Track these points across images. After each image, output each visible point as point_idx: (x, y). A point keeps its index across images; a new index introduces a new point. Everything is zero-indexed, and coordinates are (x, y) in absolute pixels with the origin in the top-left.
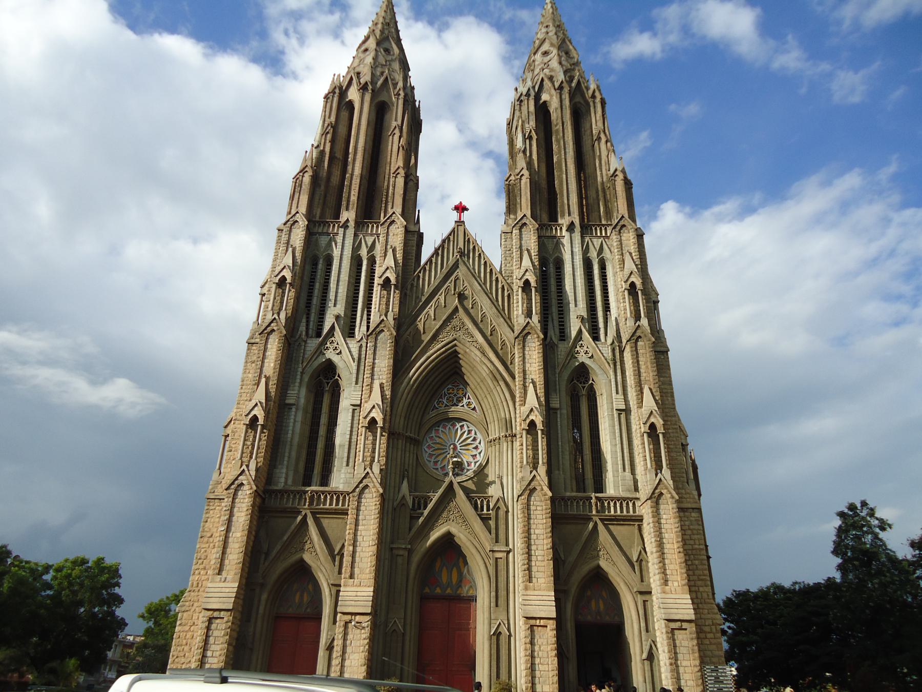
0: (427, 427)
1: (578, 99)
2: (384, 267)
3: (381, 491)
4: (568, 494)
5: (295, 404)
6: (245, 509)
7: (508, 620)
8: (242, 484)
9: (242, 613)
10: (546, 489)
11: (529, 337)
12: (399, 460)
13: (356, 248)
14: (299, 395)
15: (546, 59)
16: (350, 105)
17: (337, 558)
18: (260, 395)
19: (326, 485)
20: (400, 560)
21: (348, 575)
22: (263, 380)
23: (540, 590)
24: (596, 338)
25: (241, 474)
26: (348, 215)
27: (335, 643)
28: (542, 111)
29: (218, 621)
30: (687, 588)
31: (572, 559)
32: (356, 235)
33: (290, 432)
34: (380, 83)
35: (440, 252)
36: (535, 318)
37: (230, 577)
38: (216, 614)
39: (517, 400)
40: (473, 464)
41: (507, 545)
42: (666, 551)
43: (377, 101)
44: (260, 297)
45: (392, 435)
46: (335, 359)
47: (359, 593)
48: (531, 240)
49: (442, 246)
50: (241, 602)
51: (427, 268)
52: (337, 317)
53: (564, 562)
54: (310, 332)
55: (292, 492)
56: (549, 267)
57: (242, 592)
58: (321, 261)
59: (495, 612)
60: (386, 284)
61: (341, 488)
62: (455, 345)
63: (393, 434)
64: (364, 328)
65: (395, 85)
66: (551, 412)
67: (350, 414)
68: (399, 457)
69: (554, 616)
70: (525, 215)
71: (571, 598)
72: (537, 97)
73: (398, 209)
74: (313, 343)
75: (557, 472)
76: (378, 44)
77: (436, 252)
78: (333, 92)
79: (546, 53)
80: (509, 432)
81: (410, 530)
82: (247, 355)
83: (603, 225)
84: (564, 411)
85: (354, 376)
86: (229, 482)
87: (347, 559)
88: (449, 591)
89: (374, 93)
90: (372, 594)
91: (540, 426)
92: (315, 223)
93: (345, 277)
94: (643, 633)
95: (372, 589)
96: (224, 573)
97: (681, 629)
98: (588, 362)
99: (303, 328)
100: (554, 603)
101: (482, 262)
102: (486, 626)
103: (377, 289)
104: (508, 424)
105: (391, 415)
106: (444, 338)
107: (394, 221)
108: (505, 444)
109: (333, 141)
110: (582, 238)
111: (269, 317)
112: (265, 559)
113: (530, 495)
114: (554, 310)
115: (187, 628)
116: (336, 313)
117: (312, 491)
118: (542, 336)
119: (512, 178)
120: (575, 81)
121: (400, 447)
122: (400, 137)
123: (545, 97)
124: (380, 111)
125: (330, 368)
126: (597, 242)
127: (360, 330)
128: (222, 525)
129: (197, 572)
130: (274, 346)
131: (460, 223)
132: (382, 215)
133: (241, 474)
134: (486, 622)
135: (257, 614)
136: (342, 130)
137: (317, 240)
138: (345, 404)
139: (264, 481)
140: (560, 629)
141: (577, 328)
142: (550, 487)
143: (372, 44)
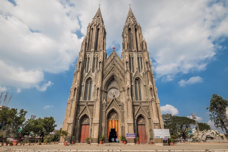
4: (135, 101)
5: (84, 85)
7: (124, 124)
8: (74, 100)
10: (131, 100)
13: (94, 56)
15: (130, 20)
18: (76, 84)
20: (104, 114)
22: (77, 81)
24: (140, 72)
26: (93, 50)
28: (130, 29)
41: (124, 110)
45: (102, 91)
46: (91, 77)
47: (96, 119)
48: (127, 54)
52: (91, 69)
58: (87, 59)
61: (93, 101)
64: (96, 71)
69: (133, 123)
72: (128, 27)
73: (102, 49)
78: (89, 26)
79: (130, 19)
81: (106, 107)
84: (134, 86)
89: (97, 27)
91: (130, 88)
93: (92, 61)
97: (156, 125)
101: (118, 58)
104: (124, 88)
106: (111, 73)
109: (89, 36)
110: (137, 53)
111: (78, 69)
114: (132, 67)
123: (130, 27)
125: (90, 78)
126: (140, 55)
127: (96, 71)
136: (91, 34)
138: (93, 85)
140: (134, 125)
143: (96, 17)
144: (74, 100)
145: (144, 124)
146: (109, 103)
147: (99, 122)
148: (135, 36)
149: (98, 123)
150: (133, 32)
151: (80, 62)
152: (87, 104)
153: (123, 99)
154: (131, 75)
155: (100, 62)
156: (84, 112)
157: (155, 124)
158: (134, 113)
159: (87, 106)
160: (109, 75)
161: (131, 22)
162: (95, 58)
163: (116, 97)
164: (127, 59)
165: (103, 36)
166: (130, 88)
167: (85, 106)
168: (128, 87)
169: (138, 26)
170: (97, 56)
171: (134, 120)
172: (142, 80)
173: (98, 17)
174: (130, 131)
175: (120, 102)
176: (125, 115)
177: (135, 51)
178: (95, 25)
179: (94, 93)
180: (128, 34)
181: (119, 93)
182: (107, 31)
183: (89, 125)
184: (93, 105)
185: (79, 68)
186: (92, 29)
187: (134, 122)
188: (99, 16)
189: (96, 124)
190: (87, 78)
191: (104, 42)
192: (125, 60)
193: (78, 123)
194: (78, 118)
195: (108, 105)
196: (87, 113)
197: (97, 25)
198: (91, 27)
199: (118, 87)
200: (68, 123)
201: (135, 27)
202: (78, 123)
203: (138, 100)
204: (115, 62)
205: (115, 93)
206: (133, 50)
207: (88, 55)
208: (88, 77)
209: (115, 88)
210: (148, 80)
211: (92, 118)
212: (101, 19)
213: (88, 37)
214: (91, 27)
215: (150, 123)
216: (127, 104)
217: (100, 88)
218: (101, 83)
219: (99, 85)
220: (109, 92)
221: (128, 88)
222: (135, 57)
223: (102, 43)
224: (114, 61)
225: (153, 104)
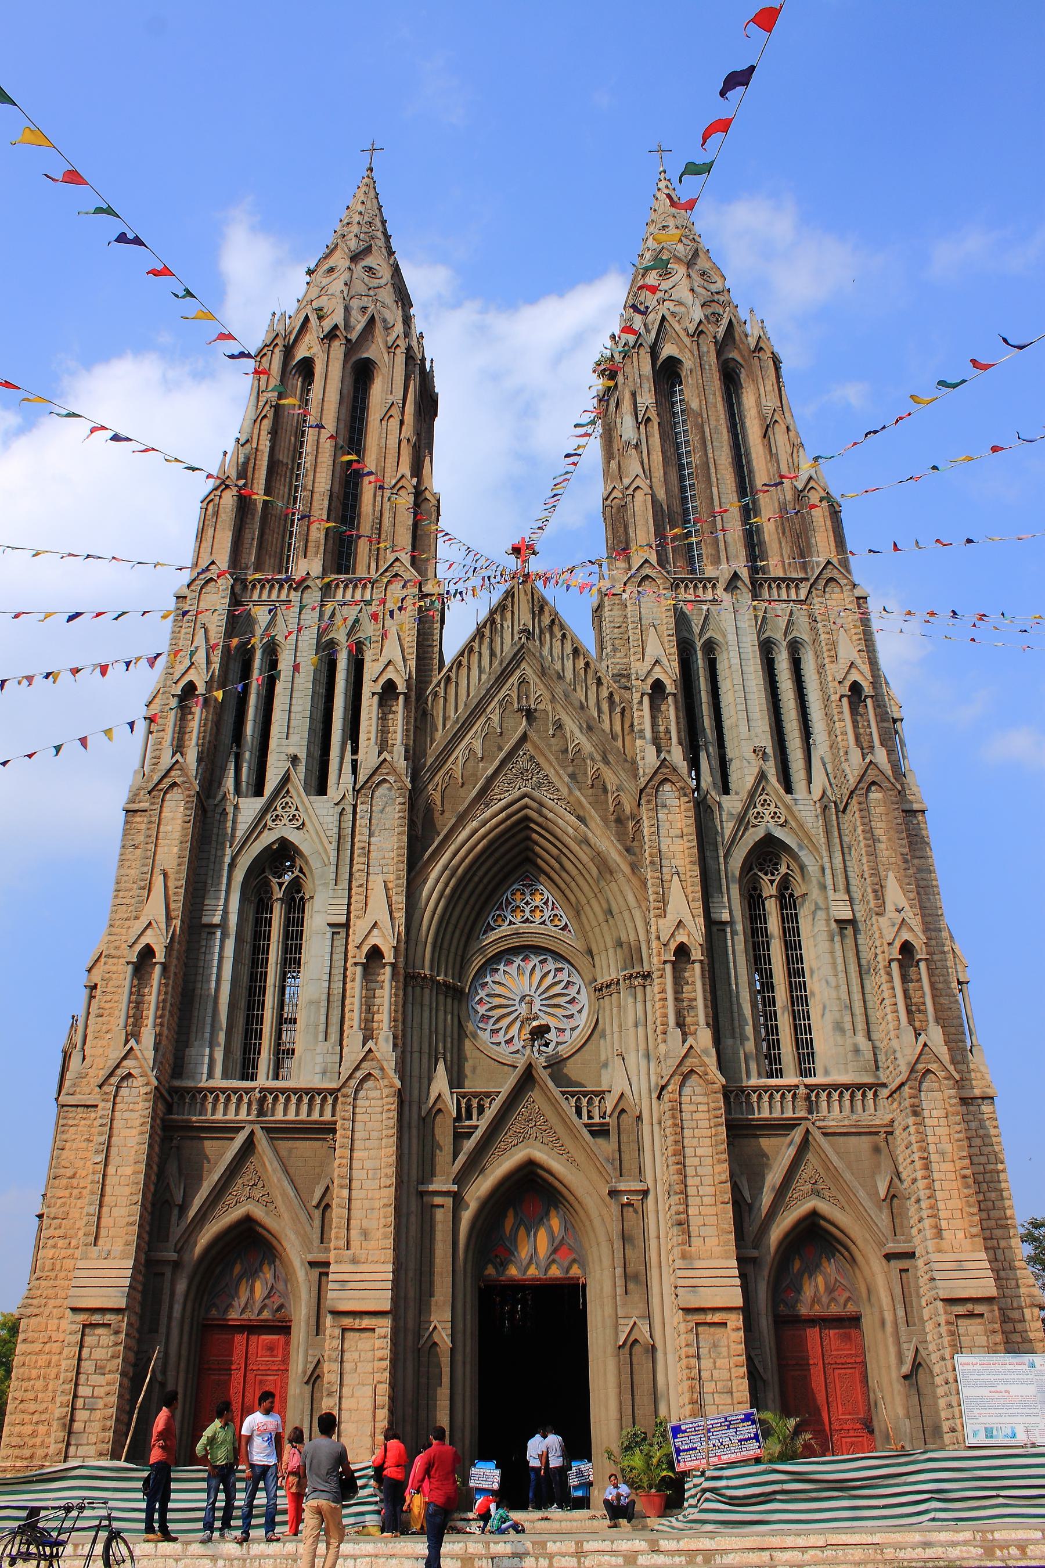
0: (478, 962)
2: (383, 660)
3: (398, 1084)
5: (223, 925)
6: (138, 1122)
9: (142, 1317)
11: (667, 787)
12: (426, 1026)
14: (227, 906)
17: (317, 1214)
18: (155, 908)
20: (439, 1214)
21: (342, 1243)
22: (159, 880)
23: (710, 1258)
24: (789, 790)
25: (125, 1058)
26: (308, 565)
27: (326, 1367)
28: (667, 374)
29: (99, 1331)
30: (979, 1240)
31: (766, 1199)
33: (214, 977)
35: (487, 631)
37: (118, 1247)
38: (97, 1318)
40: (568, 1033)
42: (936, 1176)
43: (354, 359)
45: (409, 980)
47: (366, 1273)
48: (656, 607)
49: (491, 620)
50: (139, 1296)
51: (465, 662)
52: (294, 759)
53: (750, 1206)
55: (223, 1090)
56: (696, 657)
57: (140, 1278)
59: (624, 1304)
61: (317, 1082)
62: (526, 807)
64: (347, 778)
66: (715, 928)
67: (329, 942)
68: (426, 1021)
69: (740, 1303)
70: (646, 561)
71: (766, 1272)
74: (250, 807)
75: (729, 1042)
76: (355, 258)
80: (637, 969)
81: (455, 1156)
82: (126, 833)
83: (793, 580)
84: (739, 927)
85: (333, 868)
86: (103, 1074)
87: (337, 1213)
88: (532, 1272)
89: (351, 347)
90: (390, 1276)
91: (697, 954)
93: (305, 682)
94: (903, 1327)
95: (390, 1267)
96: (101, 1242)
97: (971, 1315)
98: (779, 833)
99: (230, 782)
100: (738, 1281)
101: (569, 649)
102: (610, 1331)
103: (369, 707)
104: (632, 954)
105: (407, 942)
106: (504, 796)
109: (274, 432)
111: (167, 760)
112: (180, 1218)
113: (682, 1085)
115: (37, 1347)
116: (292, 750)
117: (262, 1090)
119: (616, 494)
120: (725, 322)
121: (426, 1001)
122: (402, 423)
123: (668, 350)
124: (361, 374)
127: (340, 782)
128: (97, 1152)
129: (51, 1242)
130: (176, 815)
132: (373, 565)
133: (125, 1058)
134: (609, 1322)
135: (170, 1317)
139: (169, 1071)
140: (749, 1326)
141: (756, 770)
142: (720, 1067)
143: (340, 260)
144: (130, 1075)
145: (851, 1308)
146: (490, 1113)
147: (394, 1300)
148: (725, 436)
149: (387, 1306)
150: (701, 391)
151: (191, 687)
152: (261, 1112)
153: (631, 1059)
154: (703, 813)
155: (390, 686)
156: (230, 1199)
157: (960, 1310)
158: (742, 1207)
159: (260, 1134)
160: (486, 821)
161: (680, 303)
162: (332, 644)
163: (564, 1040)
164: (657, 657)
165: (408, 431)
166: (697, 954)
167: (241, 1138)
168: (681, 938)
169: (752, 342)
170: (349, 635)
171: (742, 1276)
172: (812, 869)
173: (355, 258)
174: (709, 1387)
175: (601, 1094)
176: (659, 1212)
177: (736, 576)
178: (331, 335)
179: (335, 1004)
180: (653, 414)
181: (583, 998)
183: (284, 1328)
184: (330, 1129)
185: (179, 747)
186: (307, 368)
187: (745, 1288)
188: (368, 250)
189: (366, 1322)
190: (256, 848)
191: (419, 493)
192: (640, 668)
193: (177, 1308)
194: (174, 1256)
195: (482, 1123)
196: (259, 1213)
197: (354, 336)
198: (289, 351)
199: (570, 941)
200: (74, 1310)
201: (719, 353)
202: (177, 1308)
203: (780, 1074)
204: (537, 689)
205: (551, 1001)
206: (710, 572)
207: (261, 615)
208: (268, 838)
209: (538, 950)
210: (876, 873)
211: (312, 1264)
212: (385, 274)
213: (265, 445)
214: (289, 351)
215: (907, 1299)
216: (677, 1109)
217: (389, 957)
218: (400, 900)
219: (379, 924)
220: (482, 993)
221: (682, 951)
222: (732, 637)
223: (406, 500)
224: (523, 682)
225: (938, 1101)
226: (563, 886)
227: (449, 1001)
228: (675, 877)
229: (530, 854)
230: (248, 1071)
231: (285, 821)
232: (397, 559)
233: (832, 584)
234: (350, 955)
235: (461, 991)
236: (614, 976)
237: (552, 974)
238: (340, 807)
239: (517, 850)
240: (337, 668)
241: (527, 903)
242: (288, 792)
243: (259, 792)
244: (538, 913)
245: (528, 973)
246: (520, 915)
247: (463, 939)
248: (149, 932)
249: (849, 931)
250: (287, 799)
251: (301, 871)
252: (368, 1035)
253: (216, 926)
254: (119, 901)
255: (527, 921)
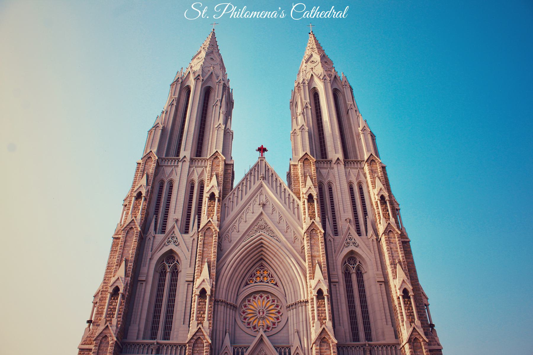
1: (335, 86)
2: (210, 186)
3: (210, 342)
16: (188, 89)
18: (121, 272)
19: (168, 339)
32: (190, 167)
34: (207, 76)
36: (318, 219)
39: (308, 275)
44: (123, 207)
46: (175, 249)
49: (250, 173)
52: (177, 221)
54: (158, 230)
58: (166, 184)
60: (212, 197)
62: (262, 239)
63: (218, 302)
65: (218, 77)
74: (160, 237)
76: (207, 55)
77: (246, 178)
78: (177, 81)
91: (325, 293)
92: (162, 159)
105: (216, 288)
107: (217, 157)
108: (300, 307)
111: (129, 220)
118: (323, 231)
122: (220, 107)
124: (207, 93)
125: (170, 256)
127: (193, 229)
131: (262, 159)
137: (164, 170)
170: (199, 178)
182: (235, 98)
203: (358, 340)
207: (168, 170)
208: (166, 249)
226: (275, 269)
227: (231, 310)
228: (317, 264)
229: (263, 257)
230: (154, 336)
231: (172, 243)
232: (217, 152)
233: (373, 162)
234: (194, 292)
235: (236, 308)
236: (294, 302)
237: (271, 301)
238: (192, 239)
239: (258, 255)
240: (195, 190)
241: (262, 275)
242: (174, 232)
243: (163, 232)
244: (265, 279)
245: (261, 301)
246: (258, 279)
247: (238, 287)
248: (118, 282)
249: (383, 285)
250: (173, 235)
251: (177, 261)
252: (200, 323)
253: (144, 281)
254: (108, 271)
255: (261, 281)
